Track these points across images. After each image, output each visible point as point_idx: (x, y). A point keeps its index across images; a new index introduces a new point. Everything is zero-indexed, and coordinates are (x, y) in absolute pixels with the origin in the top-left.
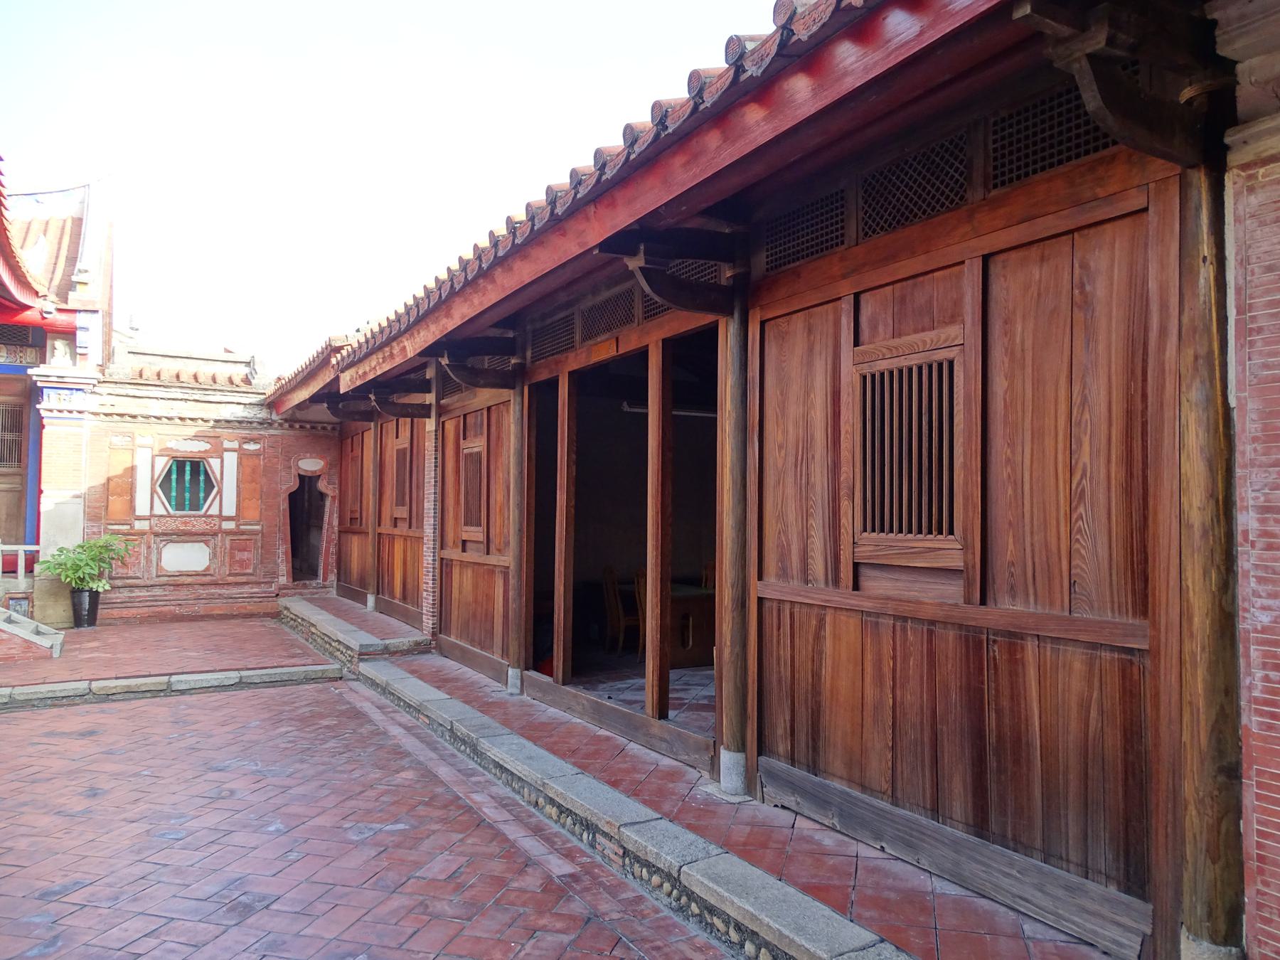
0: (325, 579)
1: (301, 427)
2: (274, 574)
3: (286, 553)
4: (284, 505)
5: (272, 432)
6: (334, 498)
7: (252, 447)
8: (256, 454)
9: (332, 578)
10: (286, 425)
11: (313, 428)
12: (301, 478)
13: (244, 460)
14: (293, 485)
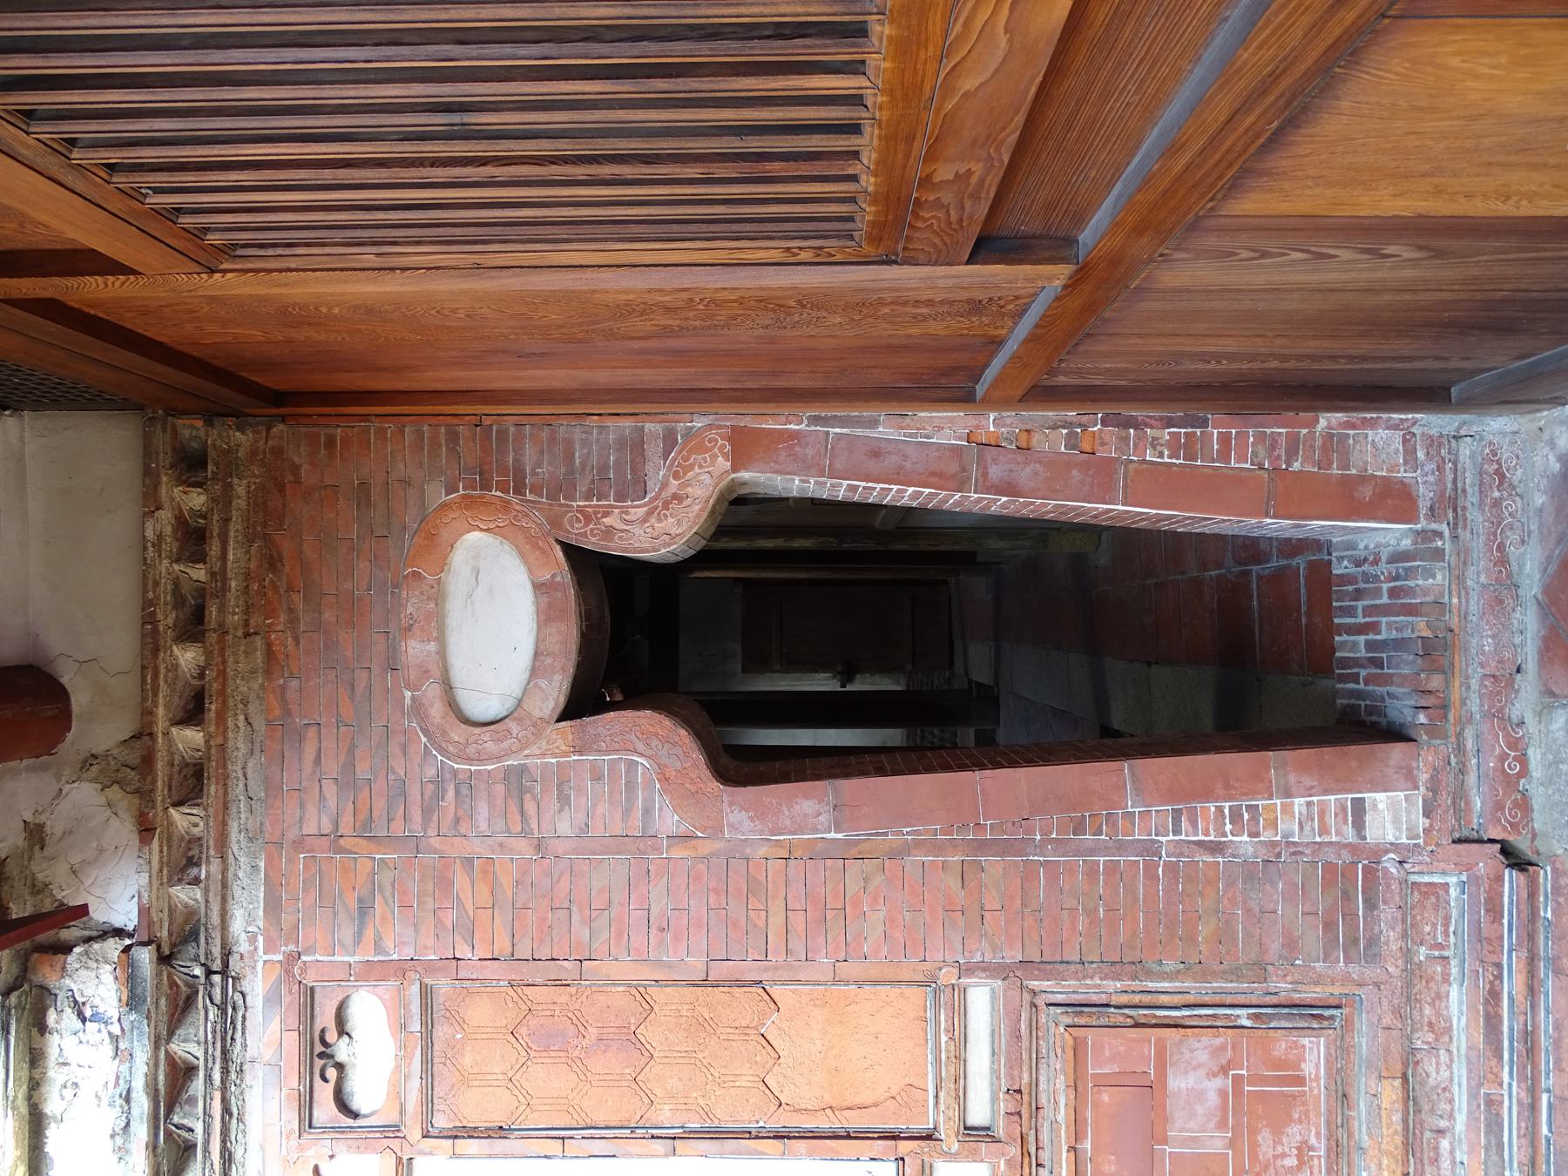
0: (1393, 500)
1: (193, 713)
2: (1352, 880)
3: (1185, 795)
4: (807, 809)
5: (246, 921)
6: (743, 447)
7: (374, 1055)
8: (426, 1026)
9: (1381, 442)
10: (182, 820)
11: (193, 626)
12: (581, 703)
13: (479, 1107)
14: (648, 751)
